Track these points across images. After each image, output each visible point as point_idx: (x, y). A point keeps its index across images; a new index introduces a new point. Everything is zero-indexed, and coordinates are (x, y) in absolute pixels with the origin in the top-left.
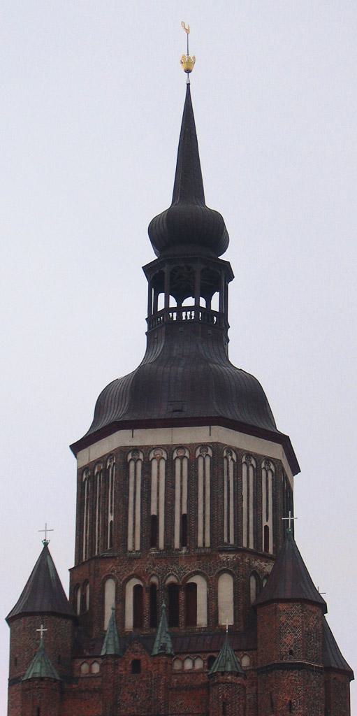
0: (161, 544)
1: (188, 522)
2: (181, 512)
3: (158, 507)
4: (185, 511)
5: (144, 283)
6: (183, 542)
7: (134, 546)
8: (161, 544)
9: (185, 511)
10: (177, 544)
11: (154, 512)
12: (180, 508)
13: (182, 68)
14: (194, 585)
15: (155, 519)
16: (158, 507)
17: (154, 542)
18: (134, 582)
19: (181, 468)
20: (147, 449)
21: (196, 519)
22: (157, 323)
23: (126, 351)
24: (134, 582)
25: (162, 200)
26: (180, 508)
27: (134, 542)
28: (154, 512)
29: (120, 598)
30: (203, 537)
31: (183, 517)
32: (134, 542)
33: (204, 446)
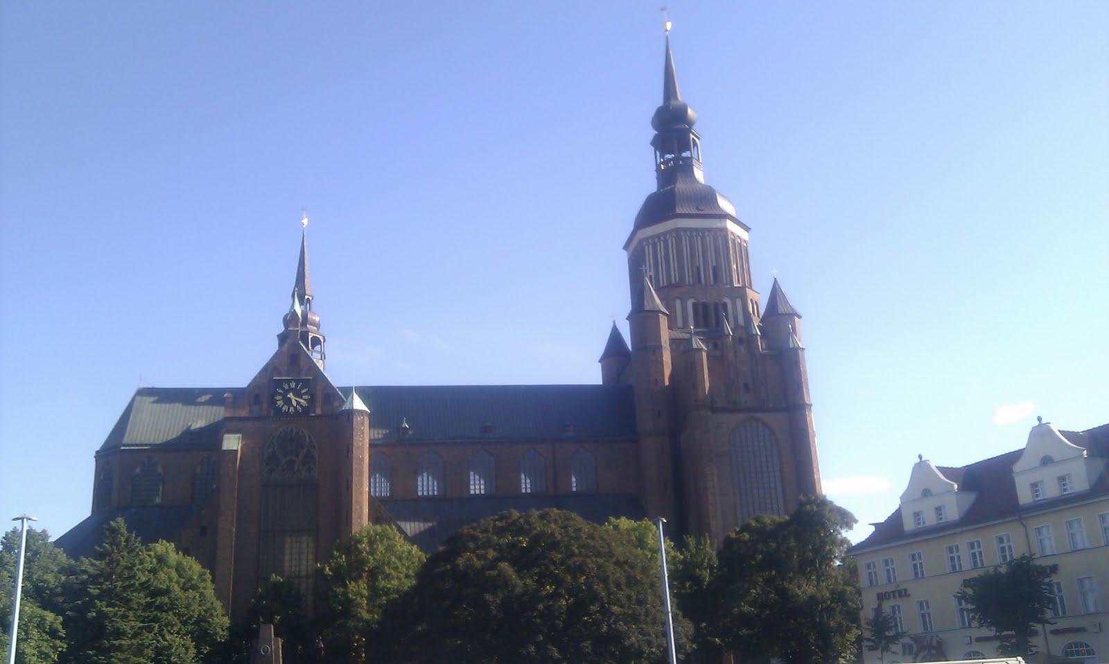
2: (712, 265)
5: (653, 148)
9: (714, 264)
10: (712, 283)
12: (712, 262)
14: (725, 305)
15: (698, 269)
23: (649, 185)
24: (693, 300)
25: (659, 101)
26: (712, 262)
27: (688, 279)
29: (684, 309)
32: (688, 279)
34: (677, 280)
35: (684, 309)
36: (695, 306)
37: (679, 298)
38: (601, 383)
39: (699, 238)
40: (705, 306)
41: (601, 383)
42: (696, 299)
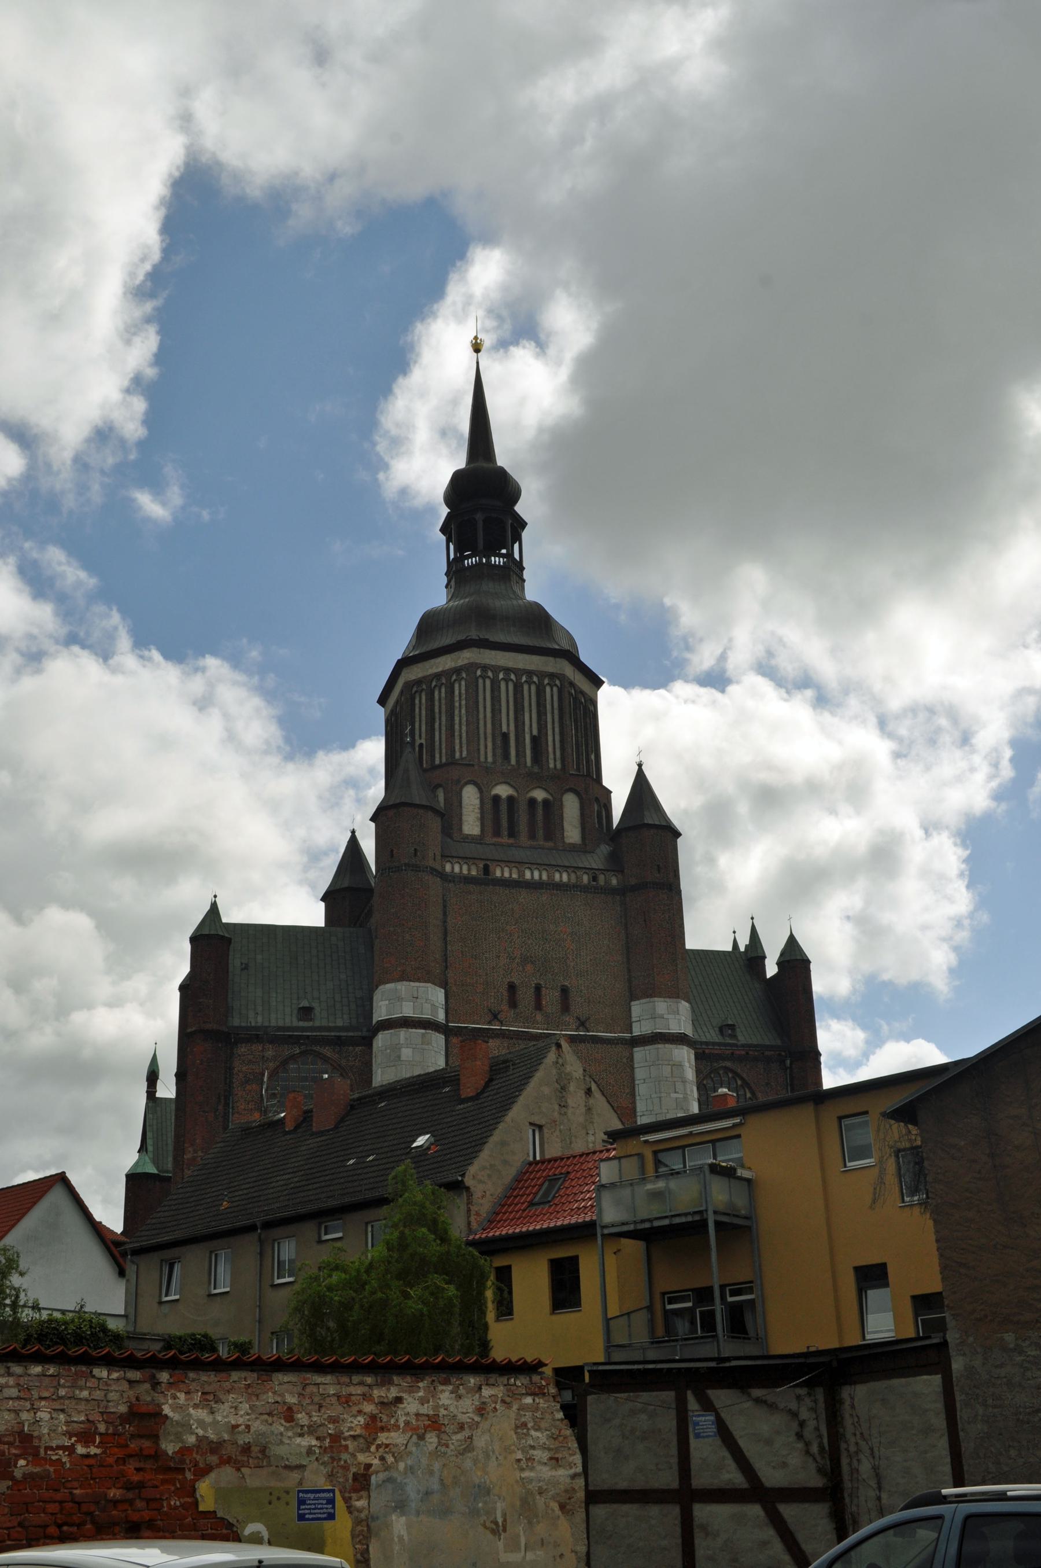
0: (513, 761)
1: (537, 742)
3: (508, 725)
7: (486, 758)
8: (513, 761)
9: (535, 732)
11: (504, 729)
13: (470, 350)
15: (505, 736)
16: (508, 725)
19: (529, 693)
20: (496, 669)
27: (488, 753)
28: (504, 729)
30: (553, 762)
31: (535, 740)
33: (552, 676)
34: (464, 754)
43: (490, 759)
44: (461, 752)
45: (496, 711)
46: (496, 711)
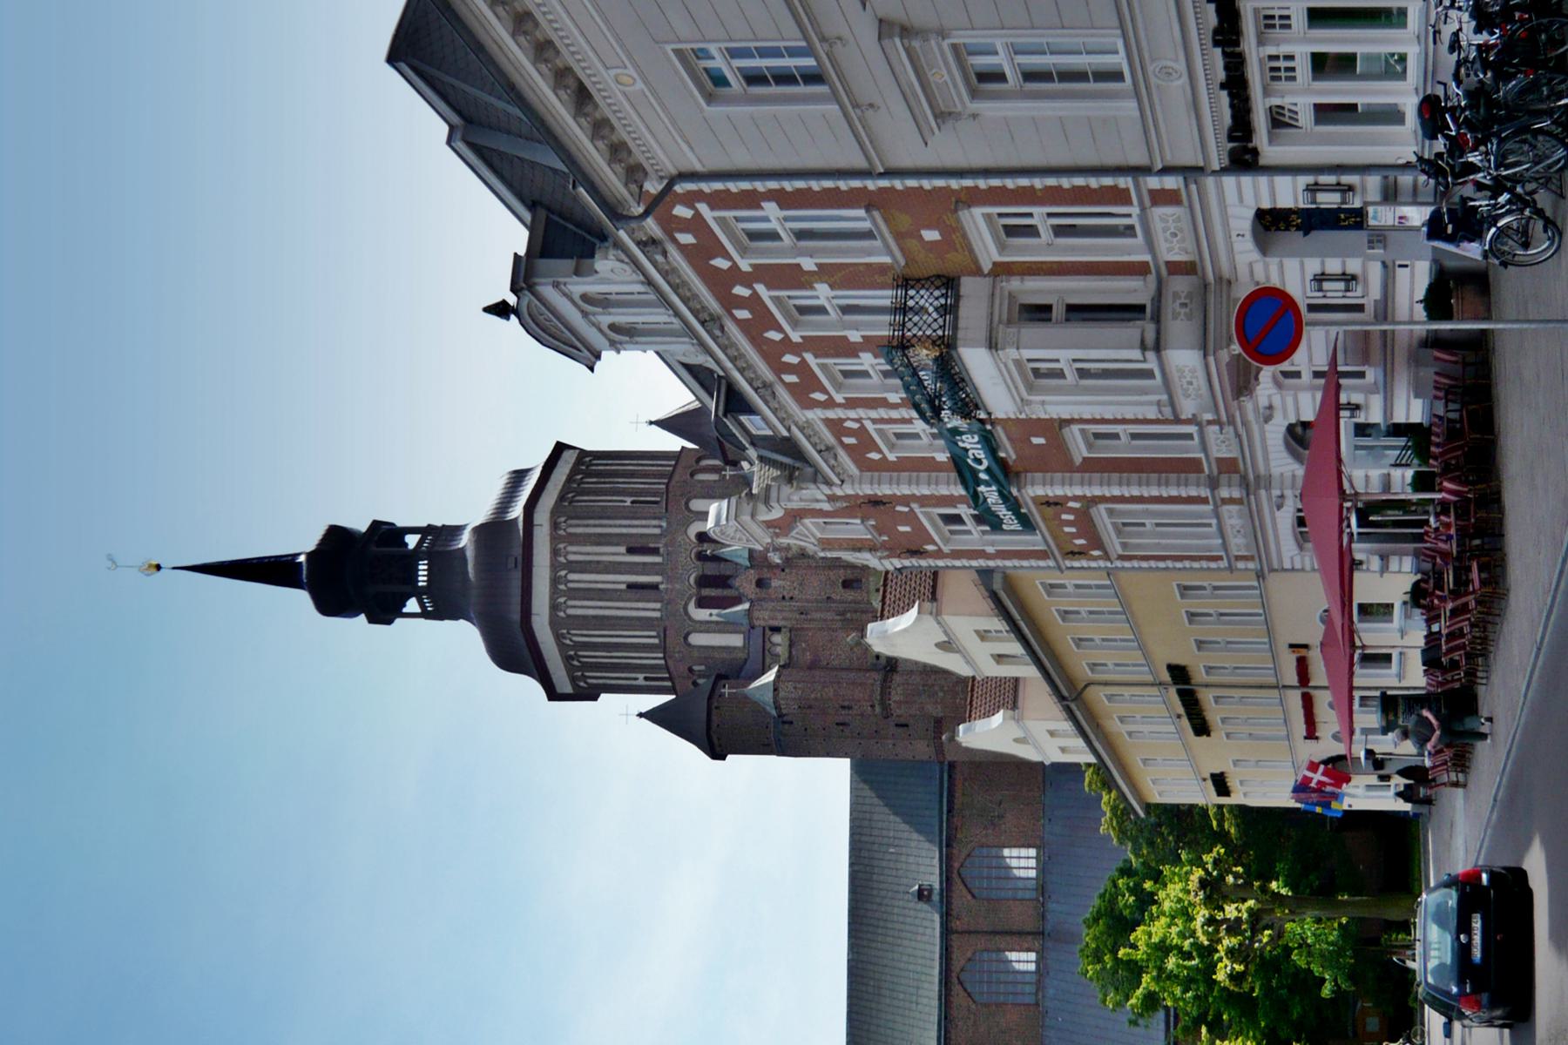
0: (656, 579)
4: (623, 549)
5: (398, 621)
6: (655, 551)
10: (658, 559)
12: (617, 553)
15: (631, 586)
17: (654, 587)
18: (692, 607)
21: (632, 535)
22: (442, 608)
24: (692, 607)
26: (617, 553)
27: (650, 609)
28: (623, 587)
29: (707, 627)
31: (631, 551)
33: (555, 526)
35: (707, 627)
36: (702, 603)
37: (686, 638)
38: (848, 761)
39: (572, 577)
40: (703, 581)
41: (848, 761)
42: (690, 599)
43: (658, 605)
44: (650, 638)
45: (602, 594)
46: (602, 594)
